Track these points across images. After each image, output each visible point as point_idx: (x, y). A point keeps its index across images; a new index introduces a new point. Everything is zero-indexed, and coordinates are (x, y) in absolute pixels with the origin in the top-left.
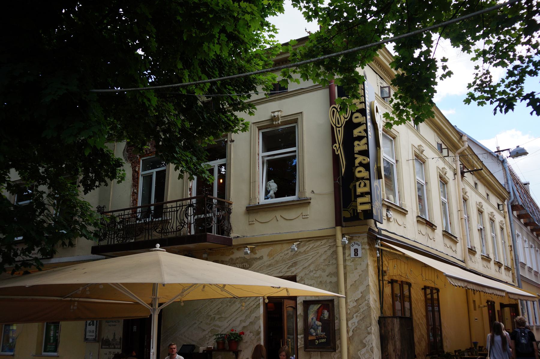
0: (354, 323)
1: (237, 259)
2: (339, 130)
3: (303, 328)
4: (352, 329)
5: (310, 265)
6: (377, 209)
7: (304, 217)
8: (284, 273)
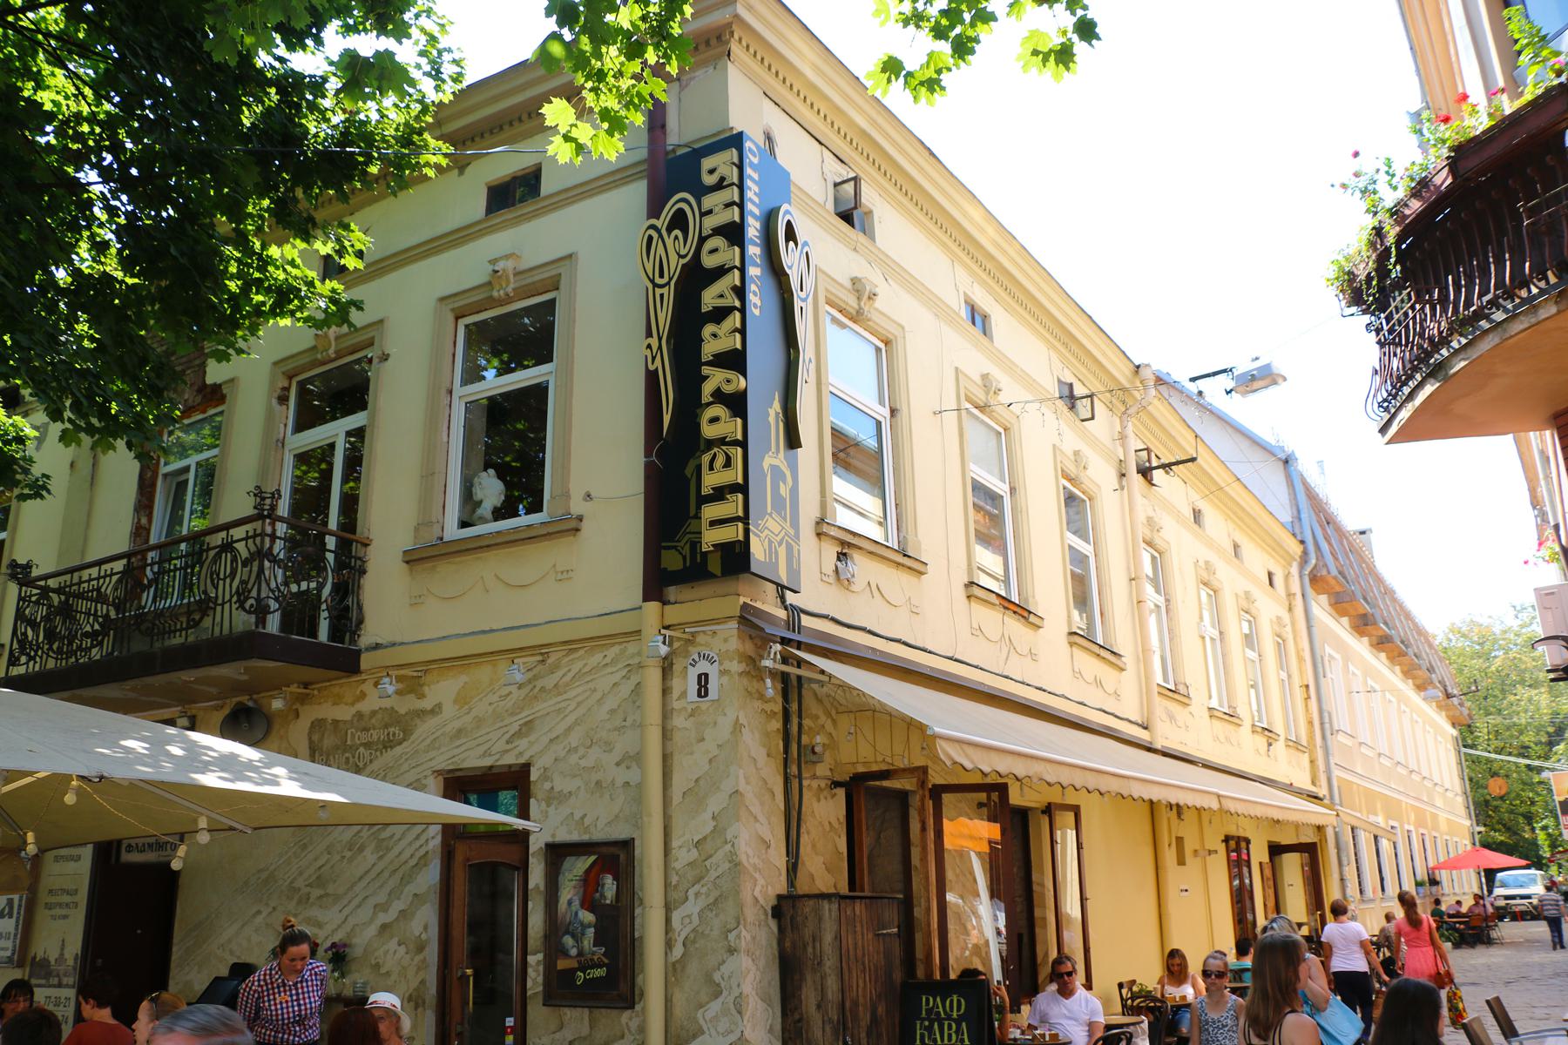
0: (689, 916)
1: (374, 713)
2: (662, 296)
3: (542, 934)
5: (569, 729)
6: (770, 542)
7: (559, 577)
8: (497, 756)
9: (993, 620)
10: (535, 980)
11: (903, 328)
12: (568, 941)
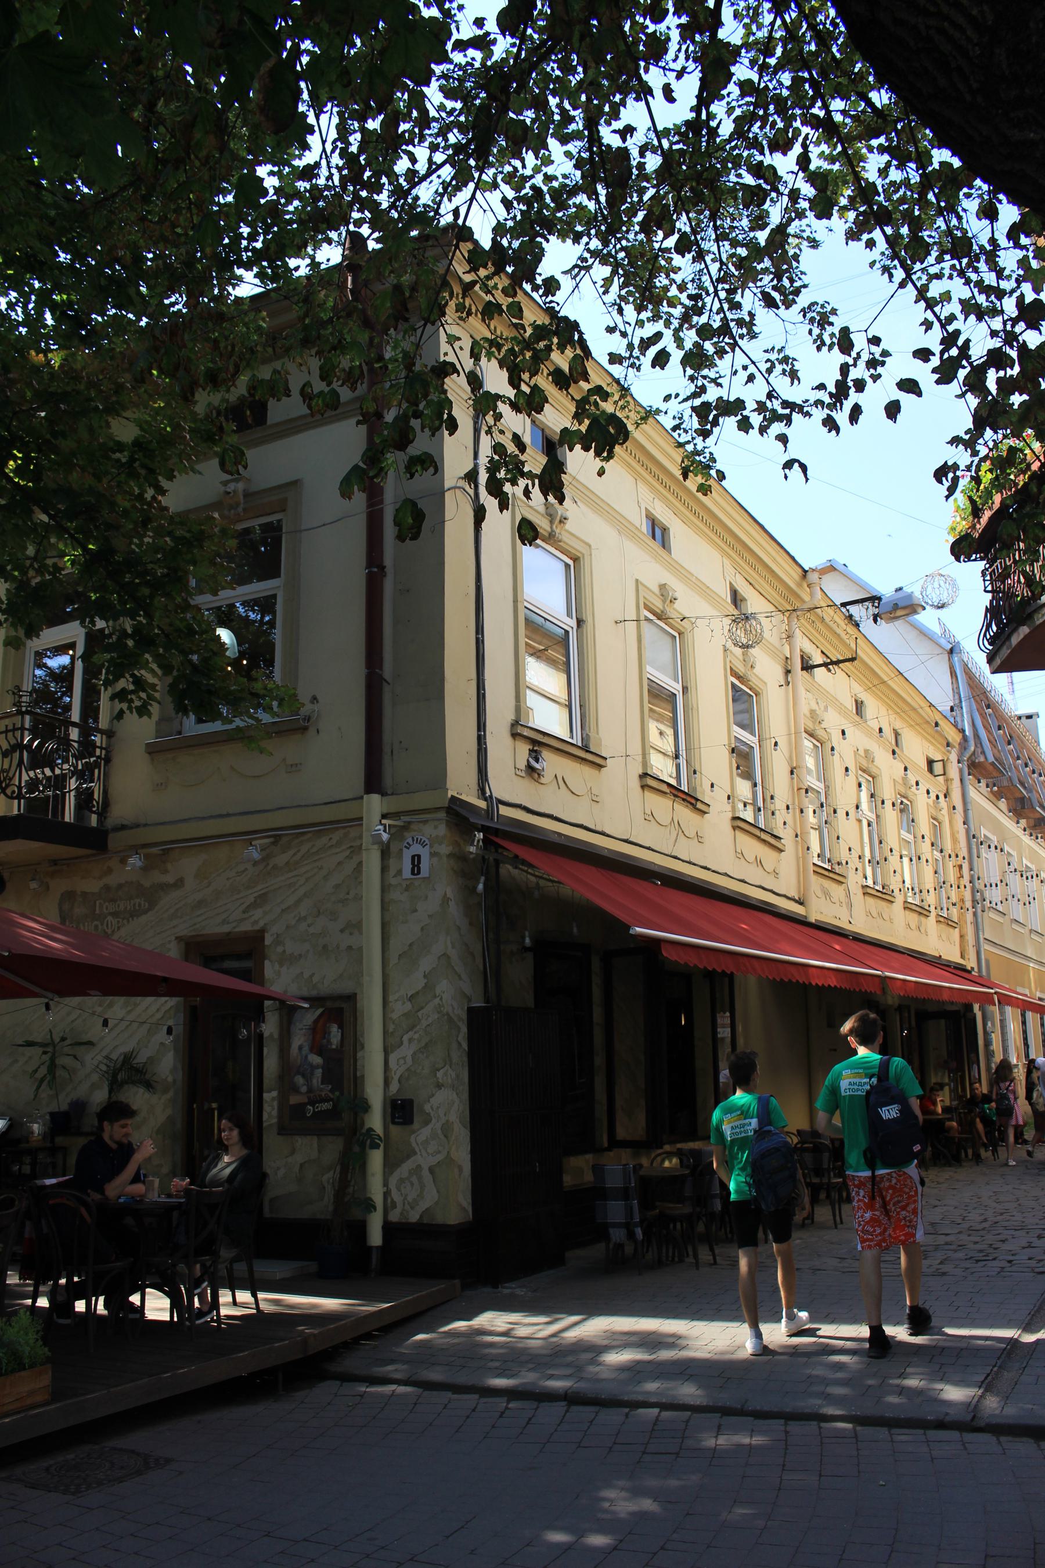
0: (404, 1058)
1: (120, 886)
4: (398, 1074)
8: (234, 924)
9: (662, 806)
10: (270, 1113)
11: (590, 546)
12: (299, 1080)
